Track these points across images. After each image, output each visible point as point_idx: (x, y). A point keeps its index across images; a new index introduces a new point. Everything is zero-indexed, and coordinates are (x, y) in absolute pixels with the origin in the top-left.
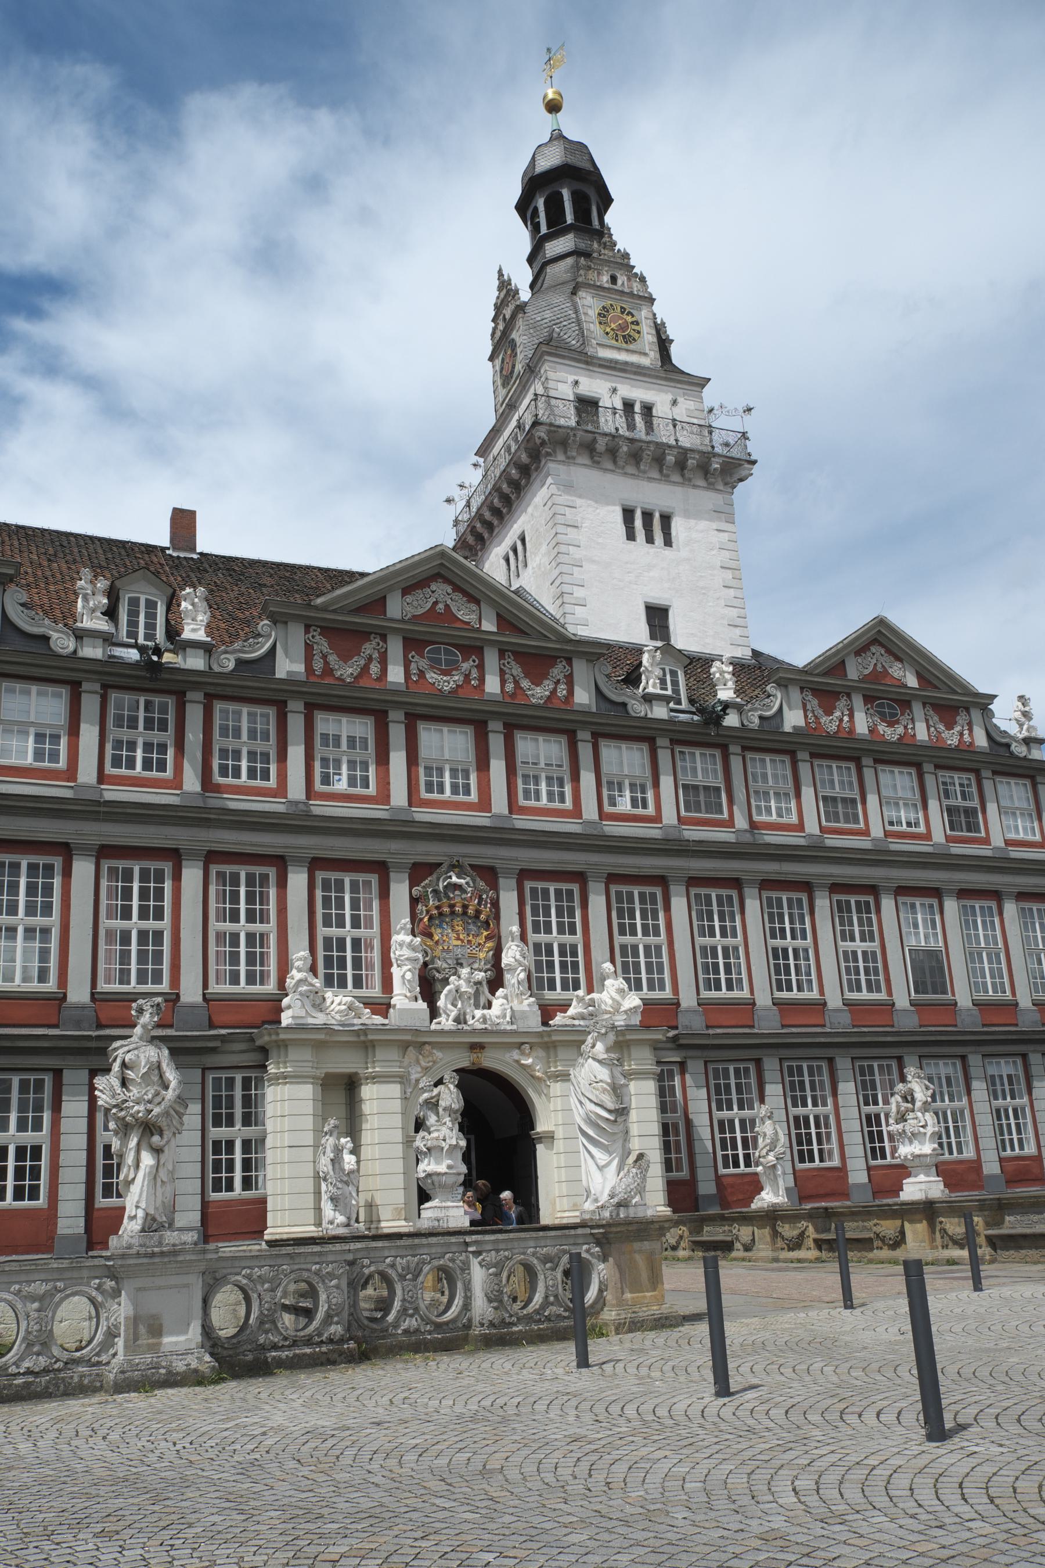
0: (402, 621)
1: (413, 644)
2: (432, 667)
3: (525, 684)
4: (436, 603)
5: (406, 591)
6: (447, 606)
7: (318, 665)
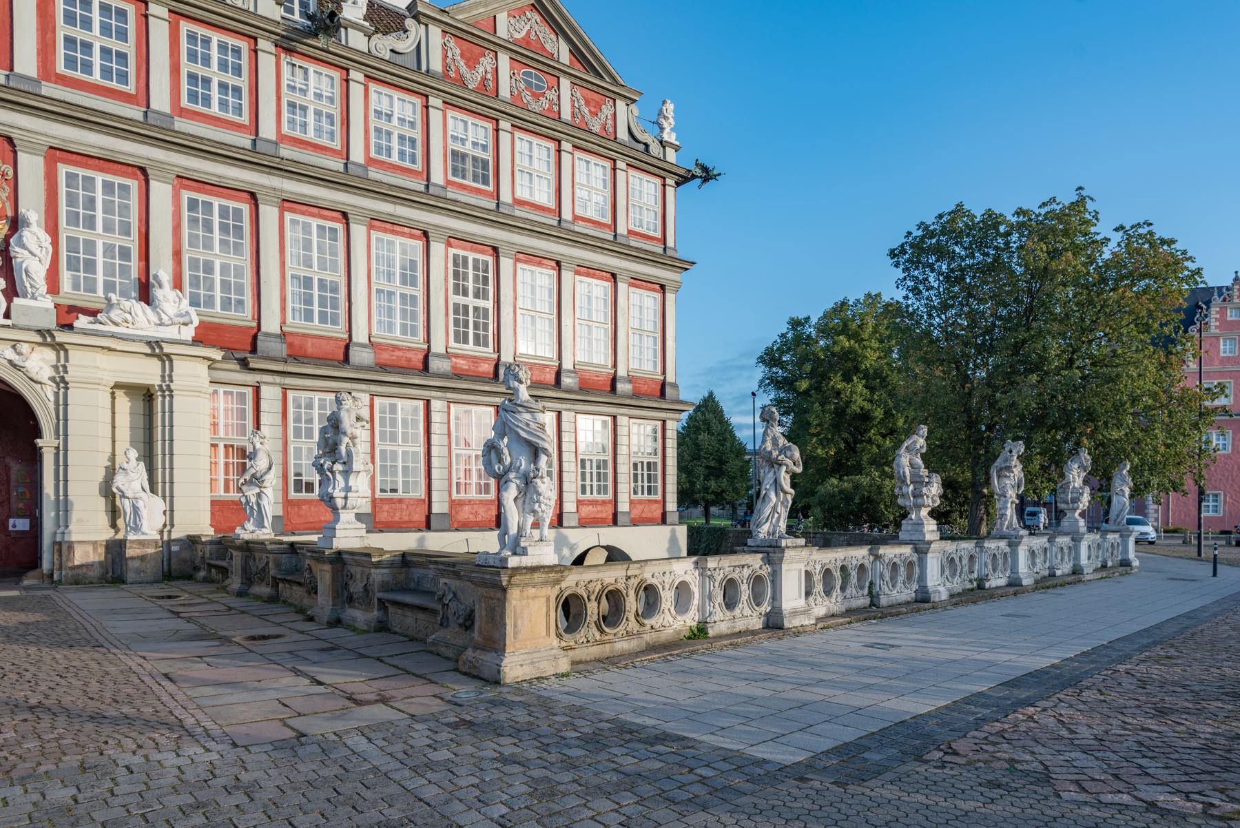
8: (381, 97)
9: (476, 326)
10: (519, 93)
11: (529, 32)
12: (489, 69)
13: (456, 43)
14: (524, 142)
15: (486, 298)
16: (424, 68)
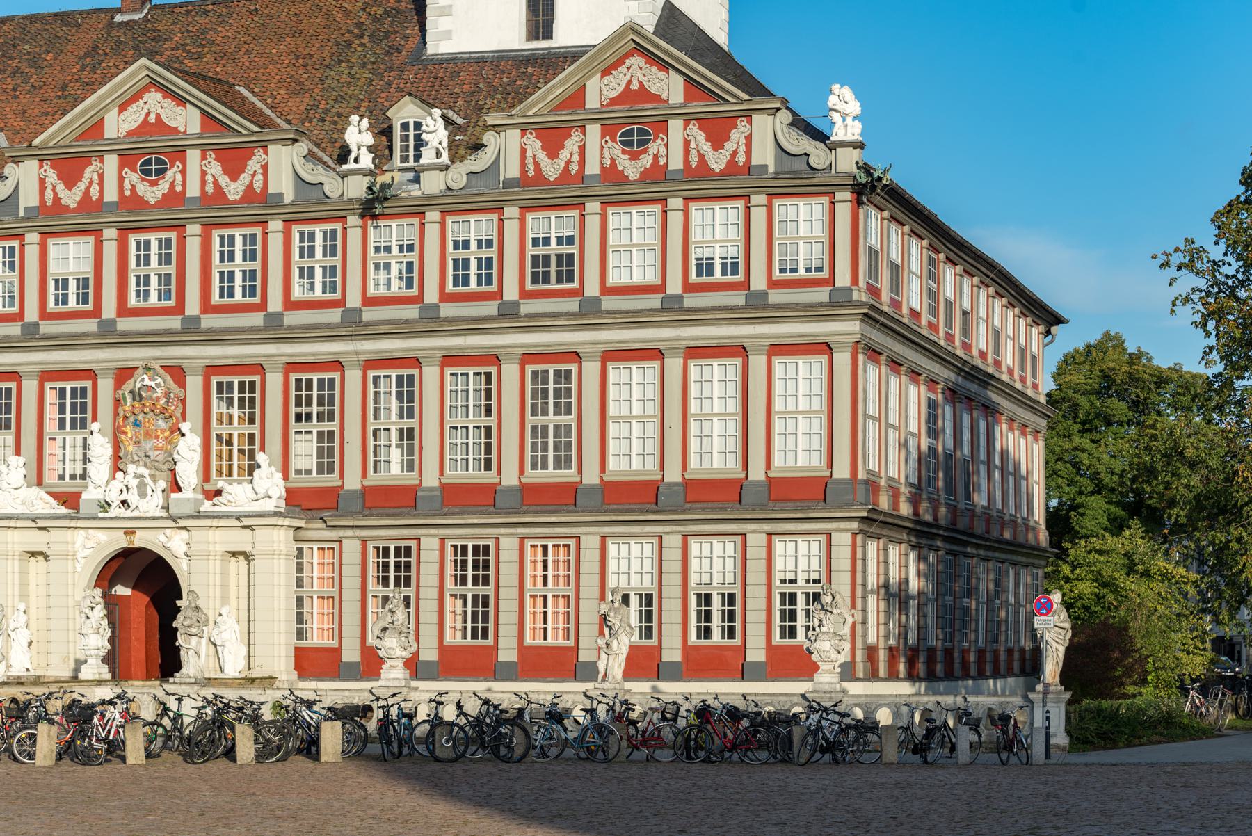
0: (116, 141)
1: (127, 159)
2: (143, 180)
3: (224, 180)
4: (148, 114)
5: (123, 108)
6: (158, 115)
7: (49, 195)
8: (459, 227)
9: (557, 447)
10: (613, 160)
11: (630, 82)
12: (576, 149)
13: (537, 137)
15: (569, 412)
16: (502, 179)
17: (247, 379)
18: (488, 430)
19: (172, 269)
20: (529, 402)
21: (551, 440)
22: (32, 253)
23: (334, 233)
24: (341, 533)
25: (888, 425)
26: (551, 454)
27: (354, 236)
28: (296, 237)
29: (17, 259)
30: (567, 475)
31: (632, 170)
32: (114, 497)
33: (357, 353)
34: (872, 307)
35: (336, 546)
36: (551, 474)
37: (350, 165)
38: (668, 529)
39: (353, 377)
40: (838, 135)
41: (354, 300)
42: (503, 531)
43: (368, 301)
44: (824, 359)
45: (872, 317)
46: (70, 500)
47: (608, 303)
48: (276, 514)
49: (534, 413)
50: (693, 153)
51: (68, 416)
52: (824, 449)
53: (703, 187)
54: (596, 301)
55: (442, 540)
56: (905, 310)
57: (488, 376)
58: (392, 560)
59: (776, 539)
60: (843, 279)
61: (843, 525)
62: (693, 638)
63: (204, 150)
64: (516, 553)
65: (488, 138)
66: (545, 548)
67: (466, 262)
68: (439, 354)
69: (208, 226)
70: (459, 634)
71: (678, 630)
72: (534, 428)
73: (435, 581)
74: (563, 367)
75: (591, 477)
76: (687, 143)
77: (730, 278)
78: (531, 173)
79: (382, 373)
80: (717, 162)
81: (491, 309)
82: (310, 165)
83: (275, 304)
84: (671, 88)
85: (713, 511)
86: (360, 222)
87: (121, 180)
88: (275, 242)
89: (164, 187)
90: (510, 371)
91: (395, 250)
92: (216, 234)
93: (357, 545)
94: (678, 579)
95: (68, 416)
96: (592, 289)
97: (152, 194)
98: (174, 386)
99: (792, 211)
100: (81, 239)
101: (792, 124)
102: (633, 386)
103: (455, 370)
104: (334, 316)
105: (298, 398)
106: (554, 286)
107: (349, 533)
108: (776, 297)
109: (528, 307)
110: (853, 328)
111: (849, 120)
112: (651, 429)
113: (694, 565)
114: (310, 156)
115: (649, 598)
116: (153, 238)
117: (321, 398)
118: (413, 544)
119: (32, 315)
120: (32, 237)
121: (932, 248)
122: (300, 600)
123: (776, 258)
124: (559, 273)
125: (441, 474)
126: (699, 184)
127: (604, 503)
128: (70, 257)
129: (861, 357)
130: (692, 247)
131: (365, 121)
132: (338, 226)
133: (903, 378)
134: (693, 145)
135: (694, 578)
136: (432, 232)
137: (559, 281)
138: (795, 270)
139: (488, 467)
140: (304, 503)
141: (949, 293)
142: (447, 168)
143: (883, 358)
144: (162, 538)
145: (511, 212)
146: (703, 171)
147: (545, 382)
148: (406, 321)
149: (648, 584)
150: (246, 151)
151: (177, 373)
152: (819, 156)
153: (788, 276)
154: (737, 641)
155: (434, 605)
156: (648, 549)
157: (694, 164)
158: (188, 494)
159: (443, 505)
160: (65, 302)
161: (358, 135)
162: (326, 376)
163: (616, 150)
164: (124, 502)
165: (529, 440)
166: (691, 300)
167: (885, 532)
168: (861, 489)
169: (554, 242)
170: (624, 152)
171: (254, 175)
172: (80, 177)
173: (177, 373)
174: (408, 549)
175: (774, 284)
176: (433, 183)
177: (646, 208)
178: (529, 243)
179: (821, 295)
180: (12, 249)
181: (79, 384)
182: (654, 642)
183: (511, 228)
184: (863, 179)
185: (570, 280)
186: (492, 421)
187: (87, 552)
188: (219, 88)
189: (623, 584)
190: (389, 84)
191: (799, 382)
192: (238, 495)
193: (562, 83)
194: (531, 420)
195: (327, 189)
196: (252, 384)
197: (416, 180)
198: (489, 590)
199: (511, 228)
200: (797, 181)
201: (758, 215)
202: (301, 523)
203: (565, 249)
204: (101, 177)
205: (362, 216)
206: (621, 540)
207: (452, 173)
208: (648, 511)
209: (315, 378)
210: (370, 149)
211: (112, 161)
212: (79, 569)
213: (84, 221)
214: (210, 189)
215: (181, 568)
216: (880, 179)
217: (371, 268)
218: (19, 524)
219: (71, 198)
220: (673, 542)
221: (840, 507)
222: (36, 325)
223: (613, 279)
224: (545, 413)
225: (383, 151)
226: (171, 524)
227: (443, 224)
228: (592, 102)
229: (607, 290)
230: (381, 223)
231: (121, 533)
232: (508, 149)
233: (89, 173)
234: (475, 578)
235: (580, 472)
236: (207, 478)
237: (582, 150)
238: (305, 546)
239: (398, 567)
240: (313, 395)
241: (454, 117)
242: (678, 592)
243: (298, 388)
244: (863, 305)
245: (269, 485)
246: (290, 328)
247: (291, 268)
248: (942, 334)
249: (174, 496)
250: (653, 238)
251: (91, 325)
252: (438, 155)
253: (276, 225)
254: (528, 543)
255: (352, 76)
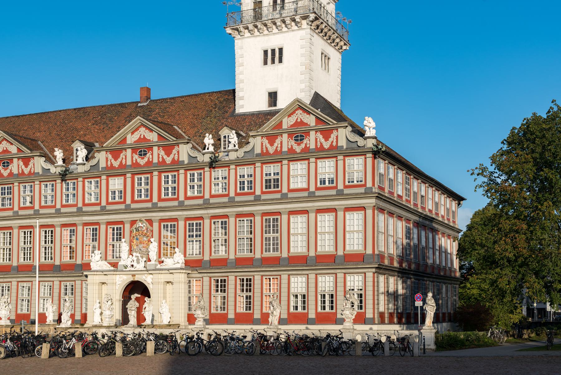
0: (130, 144)
1: (134, 150)
3: (165, 157)
5: (132, 133)
7: (109, 163)
9: (273, 245)
11: (297, 119)
12: (279, 143)
14: (293, 166)
15: (277, 233)
17: (173, 223)
18: (251, 239)
19: (149, 187)
20: (264, 229)
21: (271, 242)
22: (104, 183)
23: (201, 173)
24: (203, 275)
25: (388, 235)
26: (271, 247)
27: (207, 174)
28: (189, 175)
29: (99, 185)
30: (277, 254)
31: (298, 149)
32: (129, 264)
33: (208, 214)
34: (379, 194)
35: (201, 279)
36: (272, 254)
37: (206, 150)
38: (310, 272)
39: (207, 222)
40: (368, 134)
41: (207, 196)
42: (255, 273)
43: (212, 196)
44: (363, 212)
45: (379, 197)
46: (115, 265)
47: (290, 195)
48: (181, 269)
49: (266, 233)
50: (318, 142)
51: (115, 237)
52: (363, 244)
53: (321, 154)
54: (286, 194)
55: (236, 277)
56: (395, 195)
57: (251, 220)
58: (219, 284)
59: (347, 275)
60: (369, 184)
61: (370, 270)
62: (319, 310)
63: (159, 146)
64: (260, 281)
65: (251, 140)
66: (270, 279)
67: (244, 182)
68: (235, 214)
69: (160, 172)
70: (242, 309)
71: (314, 307)
72: (266, 238)
73: (233, 291)
74: (275, 217)
75: (285, 255)
76: (316, 139)
77: (331, 185)
78: (265, 151)
79: (216, 220)
80: (326, 145)
81: (251, 198)
82: (193, 151)
83: (182, 198)
84: (311, 120)
85: (325, 266)
86: (209, 170)
87: (132, 157)
88: (182, 177)
89: (146, 159)
90: (258, 219)
91: (220, 179)
92: (163, 175)
93: (208, 279)
94: (314, 289)
95: (115, 237)
96: (285, 190)
97: (142, 162)
98: (149, 226)
99: (352, 161)
100: (120, 178)
101: (352, 131)
102: (298, 223)
103: (240, 219)
104: (200, 201)
105: (189, 229)
106: (272, 189)
107: (206, 275)
108: (346, 191)
109: (264, 197)
110: (373, 201)
111: (371, 129)
112: (305, 238)
113: (320, 284)
114: (194, 148)
115: (304, 296)
116: (143, 177)
117: (196, 229)
118: (226, 278)
119: (104, 203)
120: (104, 177)
121: (407, 173)
122: (190, 298)
123: (347, 178)
124: (274, 185)
125: (236, 254)
126: (321, 153)
127: (289, 263)
128: (116, 184)
129: (376, 211)
130: (318, 175)
131: (211, 135)
132: (202, 171)
133: (395, 219)
134: (318, 140)
135: (319, 289)
136: (232, 172)
137: (274, 188)
138: (353, 182)
139: (251, 252)
140: (192, 265)
141: (416, 189)
142: (237, 150)
143: (386, 212)
144: (144, 277)
145: (258, 164)
146: (322, 149)
147: (270, 222)
148: (224, 203)
149: (304, 291)
150: (172, 147)
151: (150, 222)
152: (361, 142)
153: (351, 184)
154: (334, 311)
155: (233, 299)
156: (304, 279)
157: (319, 146)
158: (153, 262)
159: (236, 265)
160: (115, 199)
161: (209, 140)
162: (198, 222)
163: (292, 142)
164: (132, 266)
165: (264, 242)
166: (318, 193)
167: (387, 272)
168: (376, 257)
169: (272, 175)
170: (295, 143)
171: (175, 155)
172: (119, 157)
173: (150, 222)
174: (225, 280)
175: (346, 187)
176: (233, 156)
177: (303, 162)
178: (264, 175)
179: (362, 190)
180: (97, 181)
181: (119, 226)
182: (306, 311)
183: (258, 170)
184: (375, 149)
185: (278, 187)
186: (252, 236)
187: (120, 282)
188: (167, 127)
189: (296, 291)
190: (223, 123)
191: (354, 221)
192: (169, 263)
193: (274, 120)
194: (265, 235)
195: (198, 159)
196: (174, 225)
197: (228, 155)
198: (251, 294)
199: (258, 170)
200: (354, 151)
201: (340, 163)
202: (190, 272)
203: (276, 177)
204: (126, 156)
205: (210, 168)
206: (295, 276)
207: (239, 152)
208: (303, 266)
209: (195, 222)
210: (213, 145)
211: (129, 151)
212: (117, 288)
213: (120, 171)
214: (161, 160)
215: (150, 287)
216: (381, 149)
217: (213, 185)
218: (98, 273)
219: (116, 164)
220: (312, 276)
221: (368, 264)
222: (105, 207)
223: (292, 187)
224: (270, 233)
225: (217, 146)
226: (147, 272)
227: (236, 169)
228: (285, 126)
229: (290, 191)
230: (216, 170)
231: (131, 276)
232: (257, 143)
233: (122, 155)
234: (247, 290)
235: (281, 253)
236: (160, 257)
237: (281, 143)
238: (191, 279)
239: (222, 286)
240: (195, 227)
241: (242, 133)
242: (314, 294)
243: (189, 226)
244: (376, 193)
245: (178, 259)
246: (186, 206)
247: (187, 186)
248: (412, 203)
249: (148, 263)
250: (305, 172)
251: (122, 206)
252: (235, 146)
253: (182, 171)
254: (264, 278)
255: (211, 121)
